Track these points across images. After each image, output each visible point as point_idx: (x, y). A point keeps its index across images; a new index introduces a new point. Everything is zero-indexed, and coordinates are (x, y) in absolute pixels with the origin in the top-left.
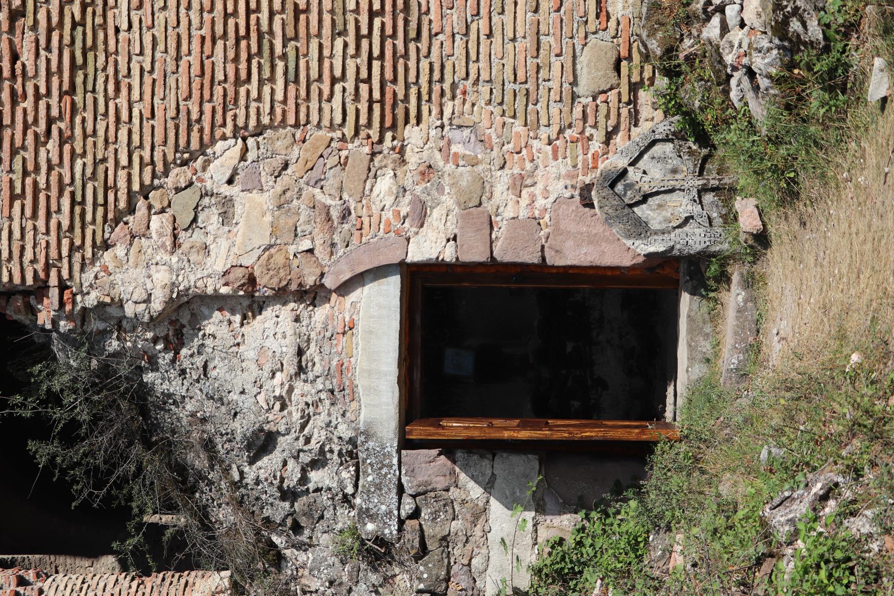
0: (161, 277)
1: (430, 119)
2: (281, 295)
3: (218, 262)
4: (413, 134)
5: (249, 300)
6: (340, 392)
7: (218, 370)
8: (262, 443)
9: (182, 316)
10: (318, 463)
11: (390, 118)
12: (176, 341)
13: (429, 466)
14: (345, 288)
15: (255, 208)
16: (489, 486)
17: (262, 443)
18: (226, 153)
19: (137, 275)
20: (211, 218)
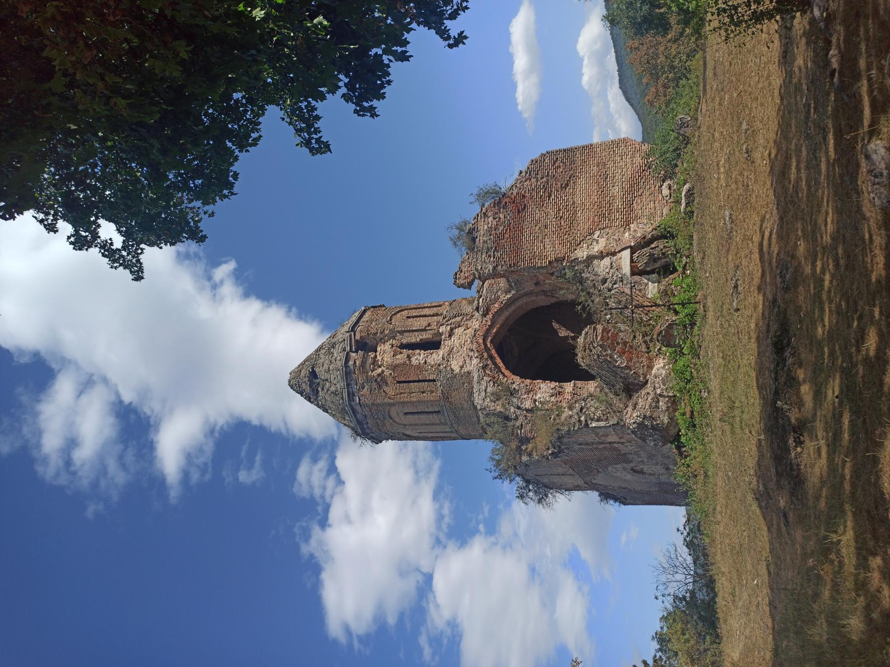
0: (585, 253)
1: (635, 223)
2: (608, 255)
3: (596, 249)
4: (632, 226)
5: (601, 256)
6: (618, 269)
7: (596, 269)
8: (604, 281)
9: (590, 259)
10: (615, 284)
11: (627, 224)
12: (588, 267)
13: (637, 278)
14: (620, 252)
15: (602, 242)
16: (648, 280)
17: (604, 281)
18: (597, 233)
19: (582, 253)
20: (595, 243)
